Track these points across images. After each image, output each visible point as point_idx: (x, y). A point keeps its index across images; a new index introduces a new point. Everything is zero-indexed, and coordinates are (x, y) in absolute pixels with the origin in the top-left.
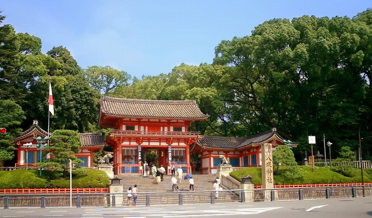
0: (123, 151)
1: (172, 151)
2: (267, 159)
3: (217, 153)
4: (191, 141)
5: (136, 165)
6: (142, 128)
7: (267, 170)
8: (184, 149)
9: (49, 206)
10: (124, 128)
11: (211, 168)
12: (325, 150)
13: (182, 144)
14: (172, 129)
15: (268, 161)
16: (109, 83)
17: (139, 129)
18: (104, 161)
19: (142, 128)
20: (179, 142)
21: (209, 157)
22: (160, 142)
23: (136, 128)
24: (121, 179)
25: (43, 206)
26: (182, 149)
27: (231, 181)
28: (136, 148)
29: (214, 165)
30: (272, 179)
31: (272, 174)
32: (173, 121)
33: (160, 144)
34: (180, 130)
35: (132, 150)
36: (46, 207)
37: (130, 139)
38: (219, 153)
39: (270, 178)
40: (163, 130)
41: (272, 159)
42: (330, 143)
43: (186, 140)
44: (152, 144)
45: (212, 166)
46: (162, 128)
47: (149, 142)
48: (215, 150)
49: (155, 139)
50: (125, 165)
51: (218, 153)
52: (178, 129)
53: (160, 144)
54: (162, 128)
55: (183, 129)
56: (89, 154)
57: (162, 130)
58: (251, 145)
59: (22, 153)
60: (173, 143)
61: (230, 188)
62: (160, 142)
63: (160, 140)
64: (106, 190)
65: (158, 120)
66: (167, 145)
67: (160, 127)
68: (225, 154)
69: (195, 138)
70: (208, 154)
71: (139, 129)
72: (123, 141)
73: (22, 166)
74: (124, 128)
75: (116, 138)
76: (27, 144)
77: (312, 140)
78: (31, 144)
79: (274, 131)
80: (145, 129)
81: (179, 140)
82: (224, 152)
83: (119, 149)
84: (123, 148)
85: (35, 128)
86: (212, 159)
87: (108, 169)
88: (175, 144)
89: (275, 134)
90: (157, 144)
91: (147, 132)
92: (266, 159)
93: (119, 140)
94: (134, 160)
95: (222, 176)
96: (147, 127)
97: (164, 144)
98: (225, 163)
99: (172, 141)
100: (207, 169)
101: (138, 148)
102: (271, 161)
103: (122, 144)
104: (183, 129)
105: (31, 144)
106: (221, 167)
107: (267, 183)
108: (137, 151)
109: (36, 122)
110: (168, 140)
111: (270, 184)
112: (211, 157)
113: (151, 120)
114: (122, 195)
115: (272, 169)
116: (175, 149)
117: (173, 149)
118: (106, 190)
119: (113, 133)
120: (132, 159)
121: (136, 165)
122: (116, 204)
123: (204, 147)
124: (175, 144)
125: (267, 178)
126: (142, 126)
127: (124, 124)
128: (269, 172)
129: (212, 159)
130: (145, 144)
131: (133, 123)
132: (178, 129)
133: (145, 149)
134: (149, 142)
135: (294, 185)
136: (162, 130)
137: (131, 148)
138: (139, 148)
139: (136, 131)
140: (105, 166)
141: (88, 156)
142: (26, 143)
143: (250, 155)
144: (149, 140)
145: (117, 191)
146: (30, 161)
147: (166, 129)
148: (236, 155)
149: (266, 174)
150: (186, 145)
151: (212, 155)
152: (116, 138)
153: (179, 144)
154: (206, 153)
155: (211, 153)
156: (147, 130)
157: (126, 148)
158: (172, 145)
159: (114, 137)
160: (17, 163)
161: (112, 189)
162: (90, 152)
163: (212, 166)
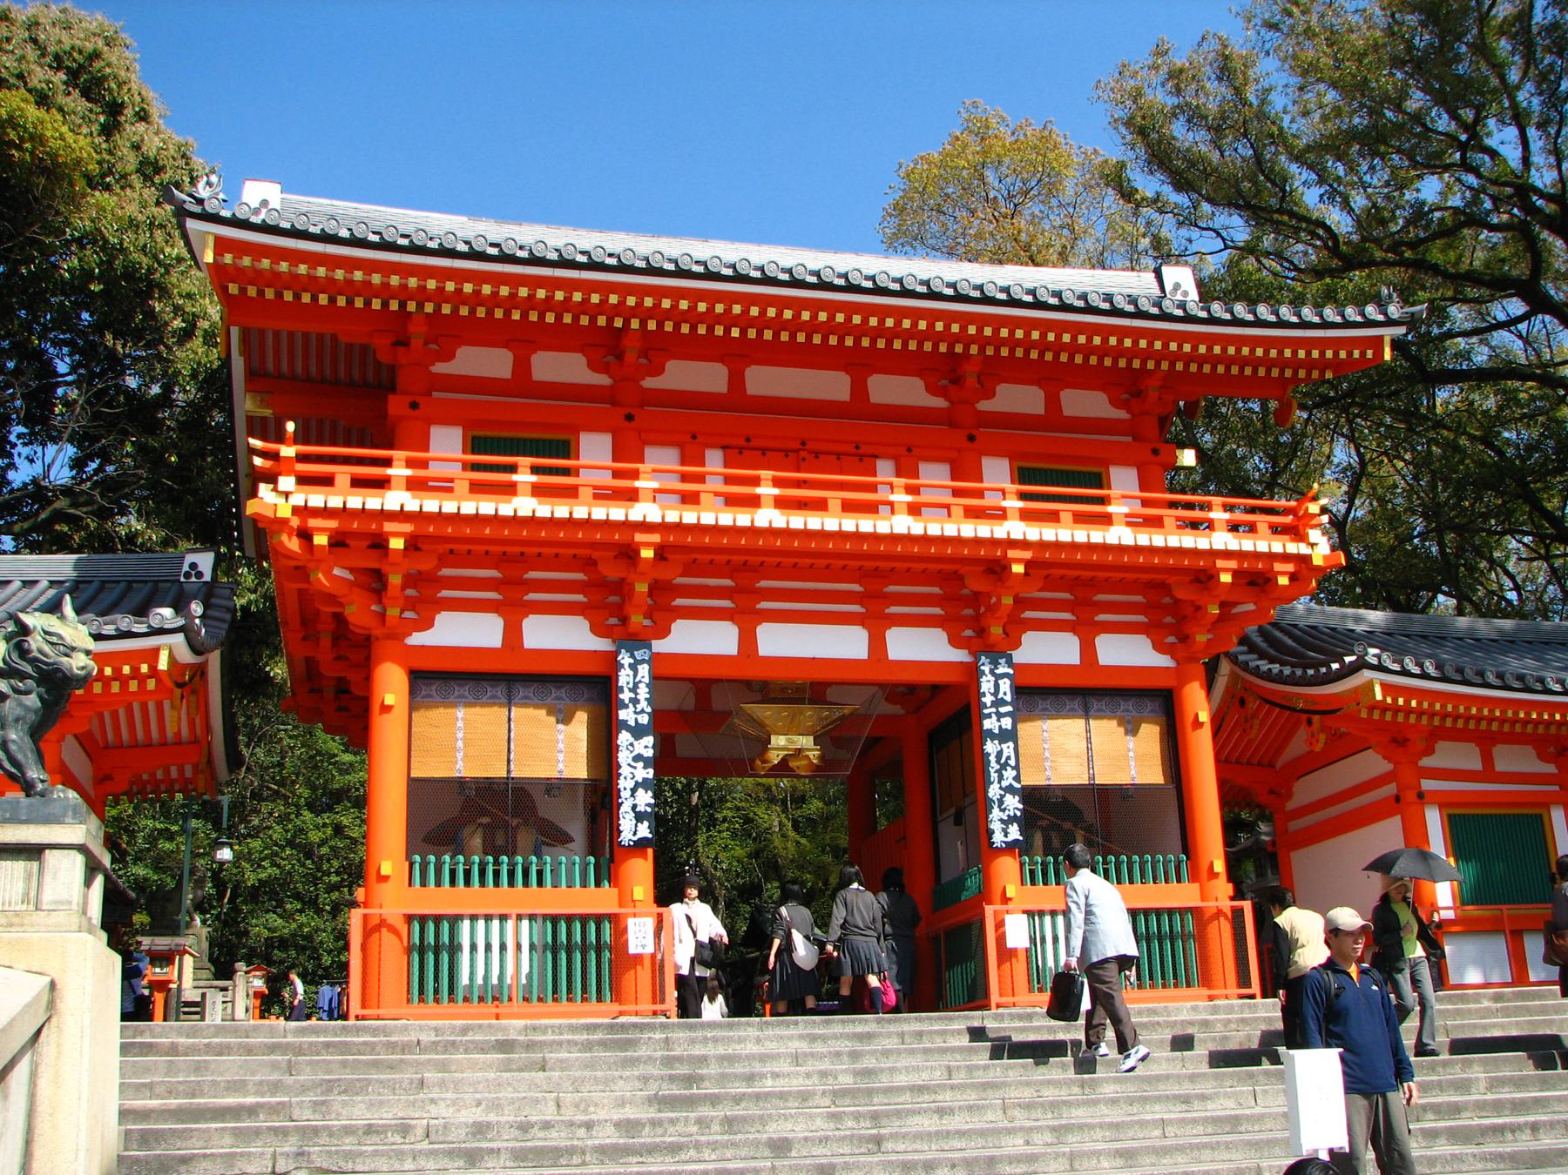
3: (1476, 764)
5: (601, 900)
13: (1126, 651)
21: (1406, 804)
38: (1501, 766)
44: (782, 641)
47: (747, 619)
51: (1487, 759)
60: (1029, 638)
67: (864, 460)
68: (1550, 768)
69: (1278, 567)
75: (321, 540)
82: (1543, 757)
86: (1434, 819)
97: (920, 646)
99: (1021, 603)
103: (417, 639)
119: (287, 482)
121: (601, 900)
123: (1367, 674)
130: (703, 638)
138: (625, 677)
150: (1164, 661)
151: (1427, 785)
152: (321, 540)
153: (1088, 650)
155: (1426, 762)
158: (1019, 656)
159: (305, 535)
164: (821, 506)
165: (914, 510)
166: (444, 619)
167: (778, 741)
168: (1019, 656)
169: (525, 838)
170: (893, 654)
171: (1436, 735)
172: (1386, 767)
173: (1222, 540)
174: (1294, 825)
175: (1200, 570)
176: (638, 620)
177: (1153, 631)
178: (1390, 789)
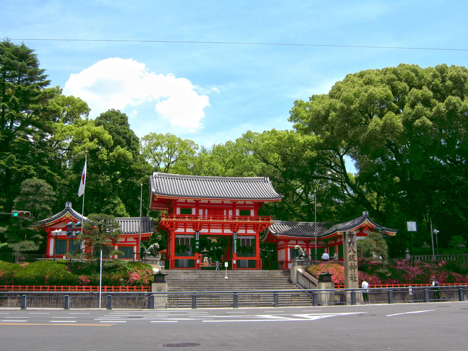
0: (177, 239)
1: (238, 240)
2: (350, 251)
4: (261, 228)
6: (201, 212)
7: (350, 265)
8: (253, 238)
9: (77, 306)
10: (178, 211)
11: (287, 262)
12: (101, 255)
13: (250, 231)
14: (238, 213)
15: (351, 253)
16: (171, 155)
17: (197, 212)
18: (149, 253)
19: (201, 212)
20: (246, 229)
22: (223, 229)
23: (194, 211)
24: (166, 275)
25: (66, 307)
26: (250, 238)
27: (308, 279)
28: (193, 237)
29: (291, 259)
30: (357, 276)
31: (356, 270)
32: (239, 202)
33: (223, 231)
34: (249, 214)
35: (187, 239)
36: (28, 309)
37: (185, 226)
39: (354, 276)
40: (227, 213)
41: (355, 250)
42: (436, 231)
43: (255, 227)
44: (213, 231)
45: (289, 259)
46: (225, 211)
47: (209, 228)
48: (293, 239)
49: (216, 226)
50: (180, 258)
52: (245, 212)
53: (223, 231)
54: (225, 211)
55: (252, 213)
56: (135, 243)
57: (225, 214)
58: (336, 233)
59: (52, 242)
61: (307, 287)
62: (223, 229)
63: (223, 226)
64: (148, 288)
65: (220, 202)
66: (232, 232)
67: (222, 210)
68: (305, 244)
70: (284, 244)
71: (197, 212)
72: (177, 228)
73: (51, 257)
74: (178, 211)
76: (56, 231)
77: (412, 226)
78: (60, 230)
79: (366, 215)
80: (204, 213)
81: (246, 226)
83: (173, 238)
84: (177, 236)
85: (68, 211)
86: (289, 249)
87: (155, 262)
88: (242, 231)
89: (367, 219)
90: (219, 231)
91: (206, 216)
92: (348, 250)
93: (172, 226)
94: (191, 251)
95: (298, 272)
96: (206, 211)
97: (228, 231)
98: (302, 256)
100: (282, 262)
101: (195, 236)
102: (355, 254)
103: (176, 231)
104: (252, 213)
105: (60, 230)
106: (297, 260)
107: (350, 282)
108: (193, 240)
109: (68, 204)
110: (234, 227)
111: (354, 283)
112: (287, 247)
113: (212, 202)
114: (166, 295)
115: (356, 263)
116: (241, 238)
117: (239, 238)
118: (148, 288)
120: (189, 250)
122: (155, 305)
124: (242, 231)
125: (349, 275)
126: (201, 208)
127: (179, 206)
128: (352, 267)
129: (289, 249)
130: (204, 231)
131: (188, 206)
132: (245, 212)
133: (203, 236)
134: (209, 228)
135: (387, 285)
136: (225, 214)
137: (187, 236)
138: (196, 235)
139: (194, 215)
140: (150, 259)
141: (134, 245)
142: (54, 229)
143: (337, 246)
144: (209, 226)
145: (161, 290)
146: (59, 252)
147: (231, 212)
148: (320, 245)
149: (349, 271)
150: (255, 233)
151: (289, 245)
154: (281, 243)
155: (289, 243)
156: (206, 213)
157: (180, 237)
158: (238, 232)
159: (166, 223)
160: (45, 253)
161: (154, 286)
162: (136, 240)
163: (289, 259)
164: (216, 219)
165: (227, 219)
166: (178, 229)
167: (213, 240)
168: (238, 232)
169: (186, 250)
170: (225, 232)
171: (289, 241)
172: (283, 243)
173: (260, 221)
174: (279, 247)
175: (258, 224)
176: (198, 229)
177: (254, 229)
178: (284, 246)
